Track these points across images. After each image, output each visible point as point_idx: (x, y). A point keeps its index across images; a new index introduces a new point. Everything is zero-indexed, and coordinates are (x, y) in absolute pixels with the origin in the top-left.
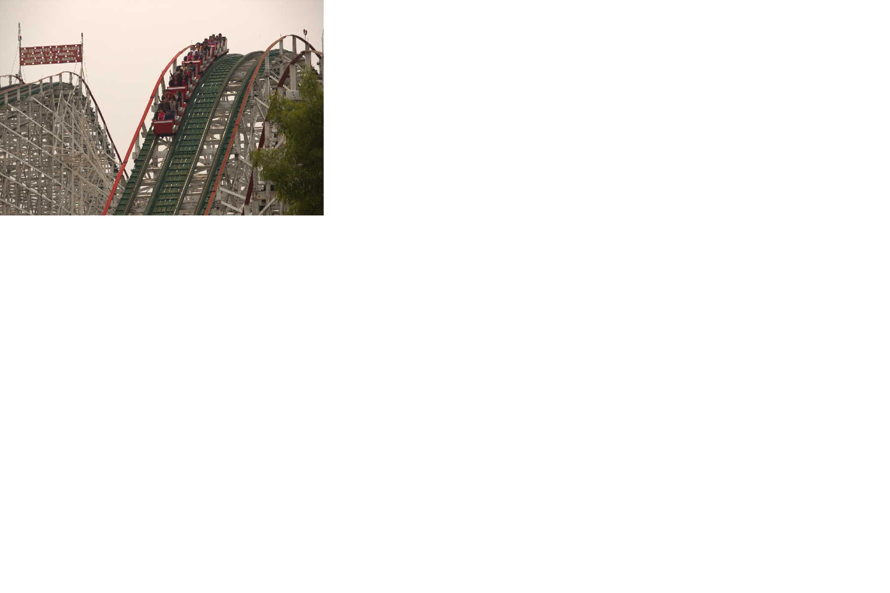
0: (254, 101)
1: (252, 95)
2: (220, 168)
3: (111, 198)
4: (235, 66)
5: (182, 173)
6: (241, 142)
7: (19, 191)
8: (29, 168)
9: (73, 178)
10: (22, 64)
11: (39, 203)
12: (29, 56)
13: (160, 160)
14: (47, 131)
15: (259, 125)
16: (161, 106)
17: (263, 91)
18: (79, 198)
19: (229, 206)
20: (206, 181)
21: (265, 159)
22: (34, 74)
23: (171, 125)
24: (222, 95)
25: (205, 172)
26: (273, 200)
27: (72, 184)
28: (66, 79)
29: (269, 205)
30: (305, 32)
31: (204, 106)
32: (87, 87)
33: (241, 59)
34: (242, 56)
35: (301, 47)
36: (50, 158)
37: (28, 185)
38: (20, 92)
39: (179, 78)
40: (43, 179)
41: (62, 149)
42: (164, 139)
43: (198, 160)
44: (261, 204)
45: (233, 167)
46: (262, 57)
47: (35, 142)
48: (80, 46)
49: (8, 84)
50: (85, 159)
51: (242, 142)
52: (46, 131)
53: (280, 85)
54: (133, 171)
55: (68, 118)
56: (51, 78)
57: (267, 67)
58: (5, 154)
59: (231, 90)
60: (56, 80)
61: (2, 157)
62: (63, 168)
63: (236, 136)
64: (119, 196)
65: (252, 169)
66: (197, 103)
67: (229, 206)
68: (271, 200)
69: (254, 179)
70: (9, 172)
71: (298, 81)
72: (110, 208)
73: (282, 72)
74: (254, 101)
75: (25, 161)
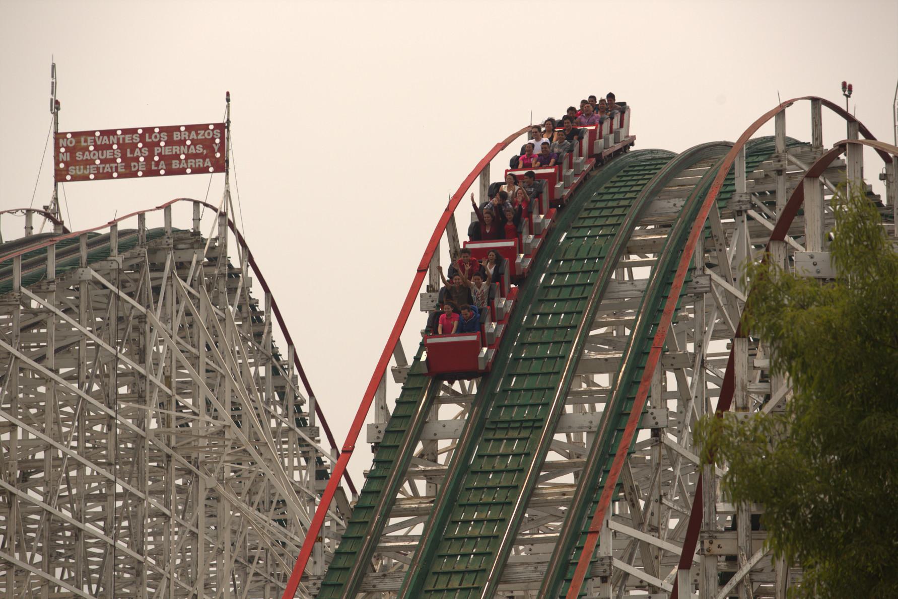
0: (704, 281)
1: (699, 264)
2: (613, 464)
3: (308, 550)
4: (651, 185)
5: (504, 480)
6: (666, 395)
7: (54, 532)
8: (80, 467)
9: (203, 495)
10: (60, 177)
11: (110, 562)
12: (82, 155)
13: (443, 444)
14: (132, 365)
15: (718, 347)
16: (447, 294)
17: (731, 251)
18: (220, 552)
19: (636, 572)
20: (570, 503)
21: (735, 440)
22: (97, 205)
23: (474, 348)
24: (616, 265)
25: (569, 478)
26: (758, 555)
27: (200, 511)
28: (182, 220)
29: (746, 568)
30: (847, 89)
31: (565, 294)
32: (241, 240)
33: (672, 163)
34: (671, 156)
35: (835, 131)
36: (138, 439)
37: (79, 516)
38: (52, 257)
39: (499, 216)
40: (118, 496)
41: (173, 413)
42: (456, 387)
43: (549, 445)
44: (723, 566)
45: (648, 464)
46: (726, 159)
47: (96, 396)
48: (223, 128)
49: (21, 234)
50: (236, 443)
51: (672, 395)
52: (127, 364)
53: (778, 236)
54: (369, 476)
55: (187, 330)
56: (141, 216)
57: (742, 184)
58: (12, 427)
59: (641, 249)
60: (154, 221)
61: (6, 437)
62: (174, 465)
63: (656, 378)
64: (330, 544)
65: (699, 469)
66: (546, 287)
67: (636, 572)
68: (750, 556)
69: (705, 499)
70: (25, 477)
71: (825, 226)
72: (305, 578)
73: (782, 201)
74: (704, 281)
75: (68, 449)
